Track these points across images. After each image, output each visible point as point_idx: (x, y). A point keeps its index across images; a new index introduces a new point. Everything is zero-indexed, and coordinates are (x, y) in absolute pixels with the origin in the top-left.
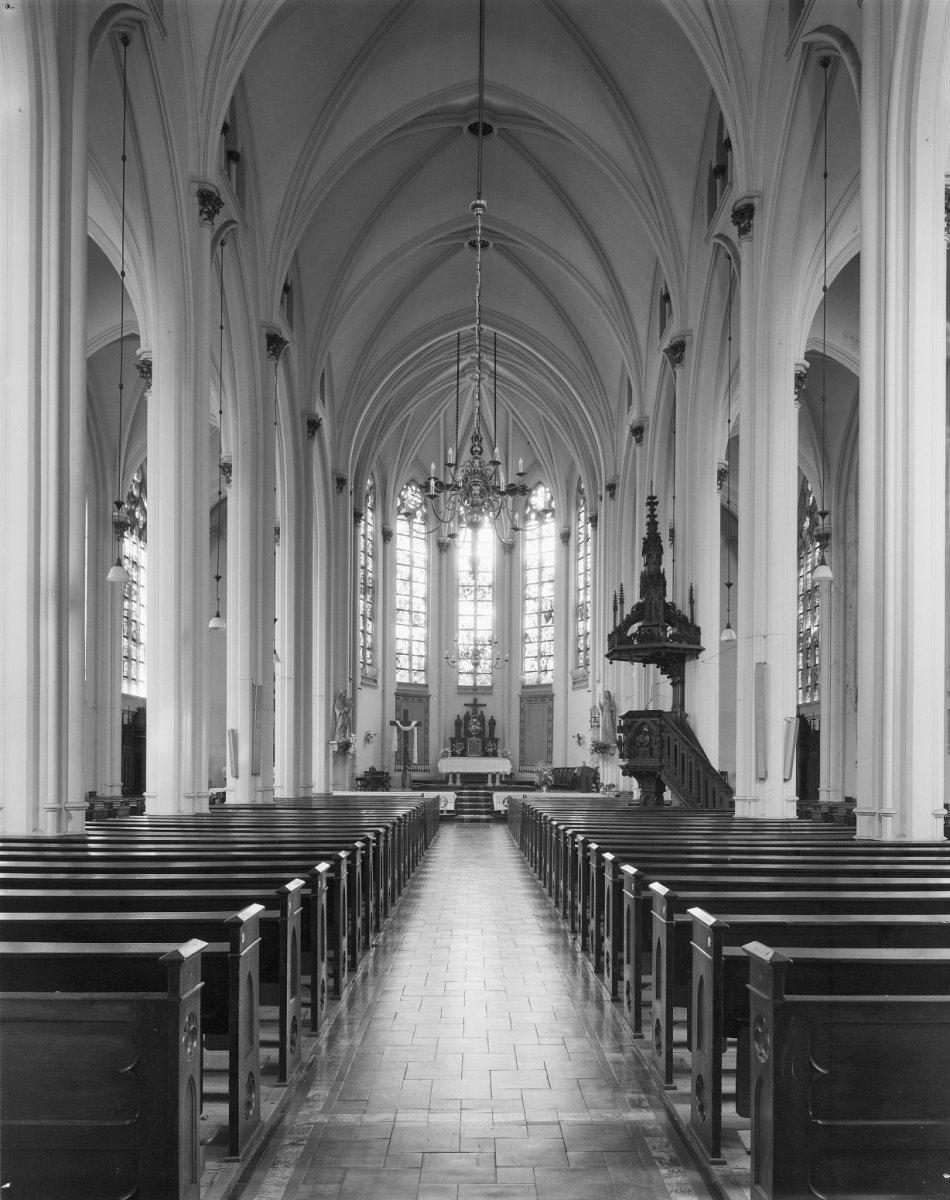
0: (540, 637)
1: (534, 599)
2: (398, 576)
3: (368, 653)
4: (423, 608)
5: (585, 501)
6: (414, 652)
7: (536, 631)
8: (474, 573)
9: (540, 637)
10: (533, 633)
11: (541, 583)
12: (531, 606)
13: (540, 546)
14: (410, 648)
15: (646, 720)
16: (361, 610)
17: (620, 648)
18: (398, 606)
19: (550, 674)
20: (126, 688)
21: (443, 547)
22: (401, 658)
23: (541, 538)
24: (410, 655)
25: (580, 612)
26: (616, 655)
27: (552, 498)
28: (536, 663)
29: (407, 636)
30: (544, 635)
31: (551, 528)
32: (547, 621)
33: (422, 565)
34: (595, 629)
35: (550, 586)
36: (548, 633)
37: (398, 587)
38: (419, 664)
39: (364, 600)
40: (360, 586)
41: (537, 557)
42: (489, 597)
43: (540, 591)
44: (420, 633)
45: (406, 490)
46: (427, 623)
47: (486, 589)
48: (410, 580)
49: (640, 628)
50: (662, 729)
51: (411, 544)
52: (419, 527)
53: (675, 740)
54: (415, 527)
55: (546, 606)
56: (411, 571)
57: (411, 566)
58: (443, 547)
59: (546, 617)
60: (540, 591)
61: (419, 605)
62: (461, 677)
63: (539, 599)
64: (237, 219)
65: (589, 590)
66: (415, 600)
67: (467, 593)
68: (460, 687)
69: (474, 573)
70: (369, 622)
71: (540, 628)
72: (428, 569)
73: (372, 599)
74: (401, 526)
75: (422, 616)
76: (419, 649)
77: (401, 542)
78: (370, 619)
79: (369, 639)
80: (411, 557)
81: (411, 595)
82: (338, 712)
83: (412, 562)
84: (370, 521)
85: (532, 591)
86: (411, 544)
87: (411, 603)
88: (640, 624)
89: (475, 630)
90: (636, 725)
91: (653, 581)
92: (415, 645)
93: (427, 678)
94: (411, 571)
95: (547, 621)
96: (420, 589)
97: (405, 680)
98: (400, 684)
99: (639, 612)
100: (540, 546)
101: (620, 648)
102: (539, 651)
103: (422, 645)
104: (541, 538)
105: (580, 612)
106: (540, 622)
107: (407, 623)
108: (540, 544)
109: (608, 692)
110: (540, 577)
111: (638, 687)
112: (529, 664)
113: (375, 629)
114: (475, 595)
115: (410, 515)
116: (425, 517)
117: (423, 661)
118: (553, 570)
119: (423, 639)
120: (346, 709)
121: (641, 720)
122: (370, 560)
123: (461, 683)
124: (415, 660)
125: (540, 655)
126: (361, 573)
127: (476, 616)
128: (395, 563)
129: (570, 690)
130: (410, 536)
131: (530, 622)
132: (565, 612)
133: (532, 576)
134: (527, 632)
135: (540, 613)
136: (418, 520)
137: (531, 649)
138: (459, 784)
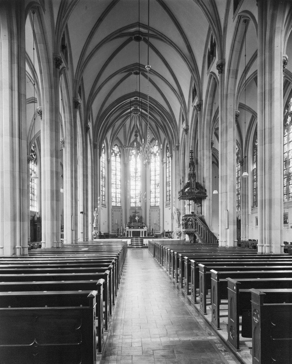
0: (155, 192)
1: (153, 180)
2: (112, 174)
3: (103, 197)
4: (120, 183)
5: (169, 151)
6: (117, 197)
8: (136, 173)
9: (155, 192)
10: (153, 190)
11: (155, 175)
12: (153, 182)
14: (116, 196)
15: (191, 217)
16: (101, 184)
17: (183, 196)
18: (112, 183)
19: (158, 203)
20: (31, 209)
21: (125, 165)
22: (113, 198)
25: (168, 184)
26: (181, 198)
27: (159, 150)
30: (156, 191)
31: (158, 158)
32: (157, 187)
33: (119, 170)
34: (175, 190)
35: (158, 176)
36: (158, 190)
37: (112, 177)
39: (102, 181)
40: (101, 177)
42: (139, 180)
43: (155, 178)
44: (119, 191)
45: (114, 147)
46: (121, 188)
47: (139, 177)
48: (116, 175)
49: (188, 190)
50: (196, 220)
51: (116, 163)
52: (118, 159)
53: (200, 223)
54: (117, 158)
55: (157, 182)
56: (116, 172)
58: (125, 165)
60: (155, 178)
61: (119, 182)
62: (132, 204)
64: (65, 66)
65: (170, 178)
66: (117, 181)
67: (133, 178)
68: (131, 207)
69: (136, 173)
70: (103, 188)
72: (121, 171)
73: (104, 181)
74: (113, 158)
75: (119, 186)
76: (119, 196)
77: (113, 163)
78: (104, 187)
79: (104, 192)
80: (116, 168)
81: (116, 179)
82: (95, 215)
83: (116, 169)
84: (103, 157)
86: (116, 163)
87: (116, 182)
88: (188, 188)
89: (135, 189)
90: (188, 219)
91: (193, 176)
92: (117, 194)
93: (121, 205)
94: (116, 172)
95: (157, 187)
96: (119, 177)
97: (114, 205)
98: (113, 206)
99: (189, 185)
101: (183, 196)
103: (120, 194)
105: (168, 184)
106: (155, 187)
108: (156, 163)
109: (177, 209)
111: (188, 207)
112: (153, 200)
113: (105, 190)
114: (136, 179)
115: (116, 155)
116: (120, 156)
118: (159, 171)
119: (120, 192)
120: (97, 214)
121: (189, 217)
122: (103, 169)
123: (131, 206)
126: (101, 173)
127: (136, 185)
128: (111, 170)
129: (165, 208)
130: (116, 161)
131: (152, 187)
132: (165, 184)
133: (153, 173)
134: (151, 190)
136: (118, 156)
137: (153, 195)
138: (132, 236)
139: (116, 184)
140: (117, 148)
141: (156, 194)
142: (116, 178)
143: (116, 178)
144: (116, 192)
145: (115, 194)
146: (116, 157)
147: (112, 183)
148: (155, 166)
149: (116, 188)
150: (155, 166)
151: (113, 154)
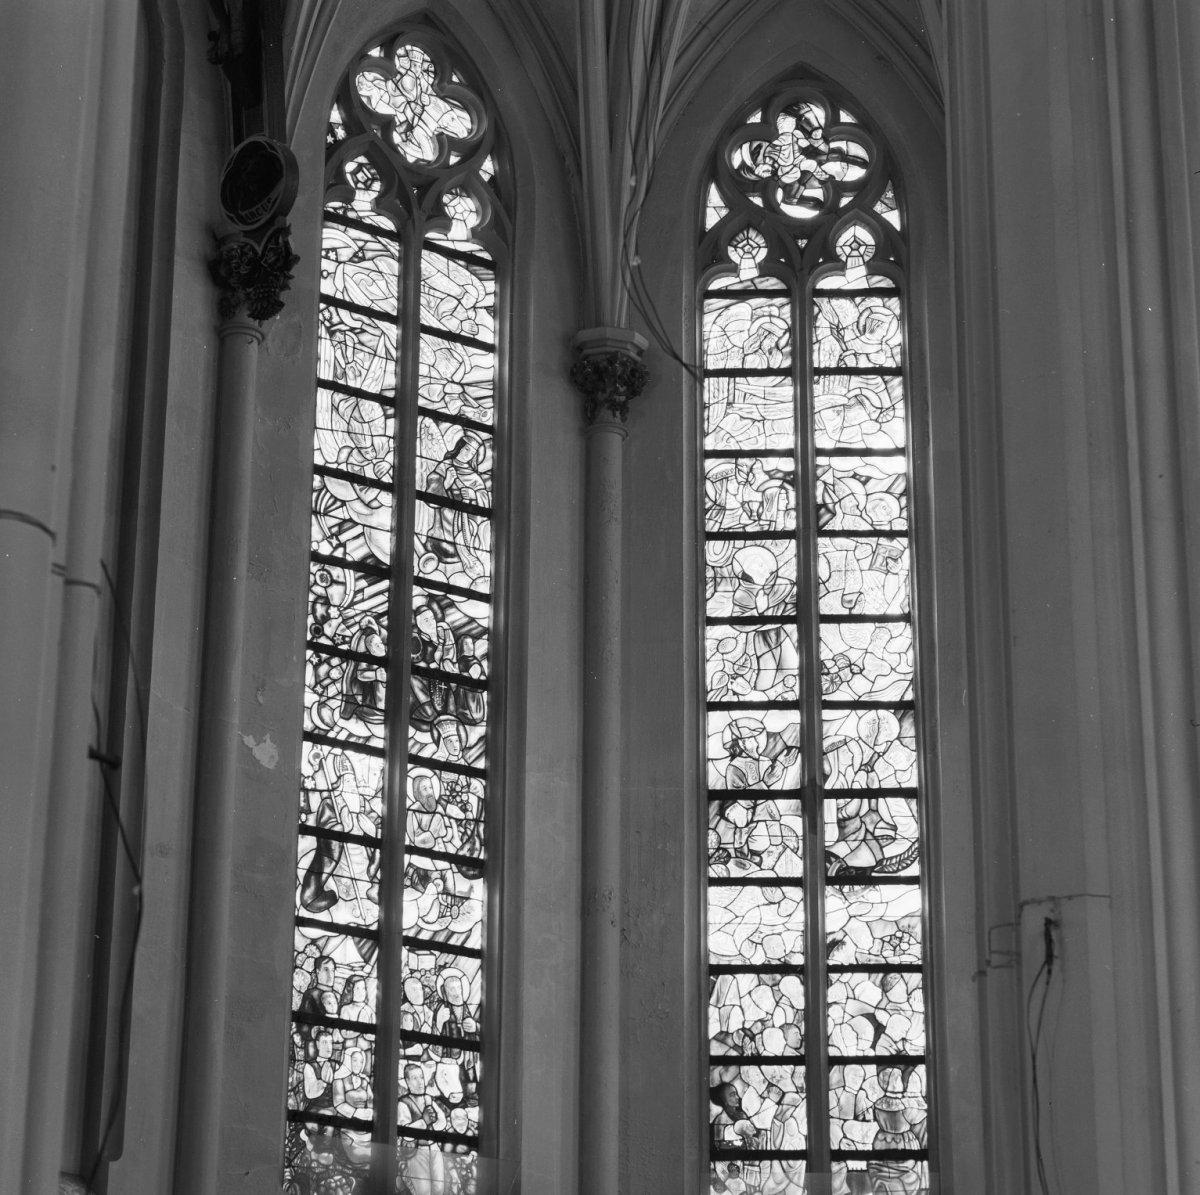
4: (902, 766)
14: (814, 1015)
24: (815, 1059)
29: (790, 945)
33: (891, 512)
38: (888, 1117)
45: (768, 132)
46: (928, 848)
56: (807, 560)
57: (811, 526)
61: (873, 748)
66: (837, 725)
75: (903, 815)
80: (802, 481)
87: (810, 746)
94: (807, 560)
96: (880, 659)
103: (908, 990)
107: (794, 867)
116: (890, 255)
117: (913, 1095)
119: (913, 954)
124: (854, 1087)
139: (810, 795)
140: (832, 130)
142: (811, 669)
143: (811, 669)
144: (818, 943)
145: (792, 986)
146: (803, 301)
147: (718, 776)
149: (824, 874)
151: (748, 259)
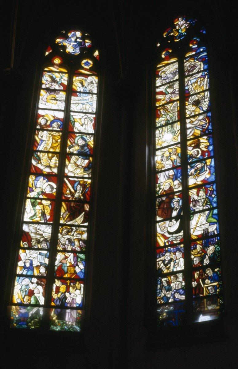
7: (47, 231)
11: (63, 156)
12: (40, 186)
13: (68, 102)
23: (70, 91)
28: (39, 291)
30: (63, 239)
32: (73, 216)
41: (61, 115)
43: (62, 166)
59: (69, 209)
60: (62, 166)
63: (59, 178)
71: (55, 223)
85: (46, 163)
100: (68, 102)
102: (50, 267)
104: (70, 91)
110: (64, 145)
125: (51, 275)
131: (33, 215)
133: (46, 140)
134: (25, 228)
135: (56, 200)
137: (31, 258)
141: (60, 256)
148: (67, 110)
150: (67, 110)
